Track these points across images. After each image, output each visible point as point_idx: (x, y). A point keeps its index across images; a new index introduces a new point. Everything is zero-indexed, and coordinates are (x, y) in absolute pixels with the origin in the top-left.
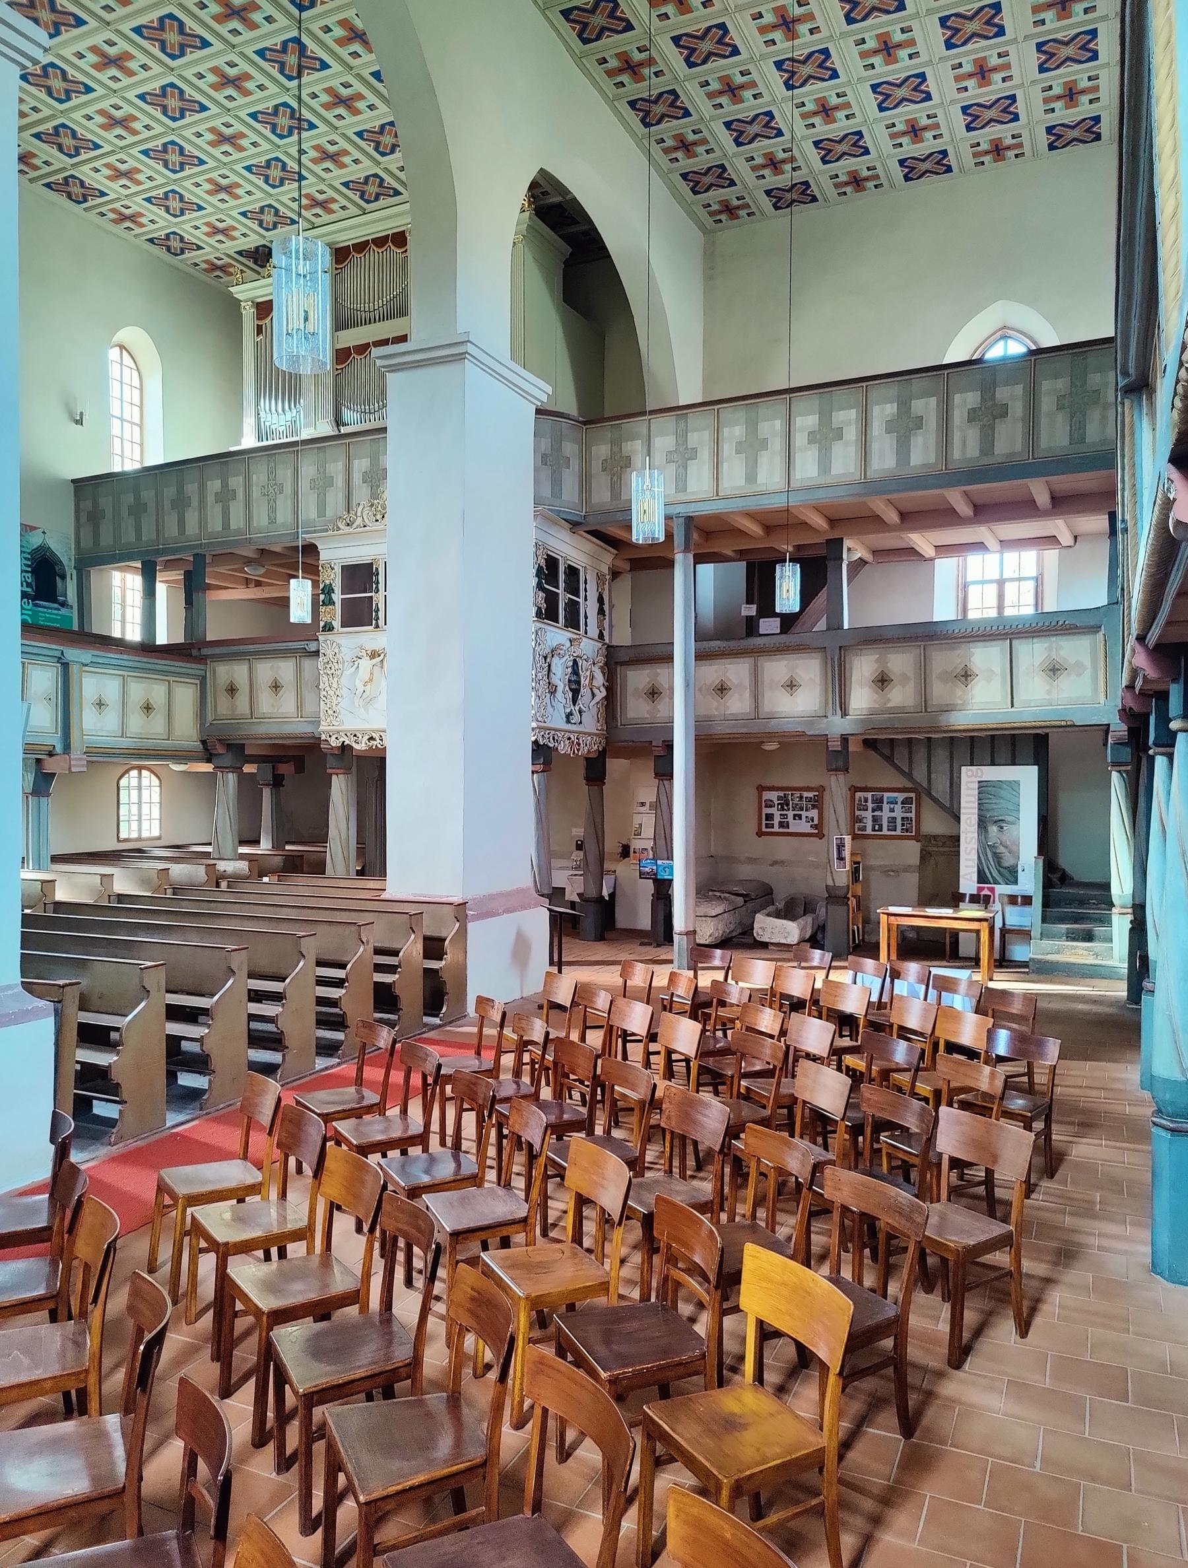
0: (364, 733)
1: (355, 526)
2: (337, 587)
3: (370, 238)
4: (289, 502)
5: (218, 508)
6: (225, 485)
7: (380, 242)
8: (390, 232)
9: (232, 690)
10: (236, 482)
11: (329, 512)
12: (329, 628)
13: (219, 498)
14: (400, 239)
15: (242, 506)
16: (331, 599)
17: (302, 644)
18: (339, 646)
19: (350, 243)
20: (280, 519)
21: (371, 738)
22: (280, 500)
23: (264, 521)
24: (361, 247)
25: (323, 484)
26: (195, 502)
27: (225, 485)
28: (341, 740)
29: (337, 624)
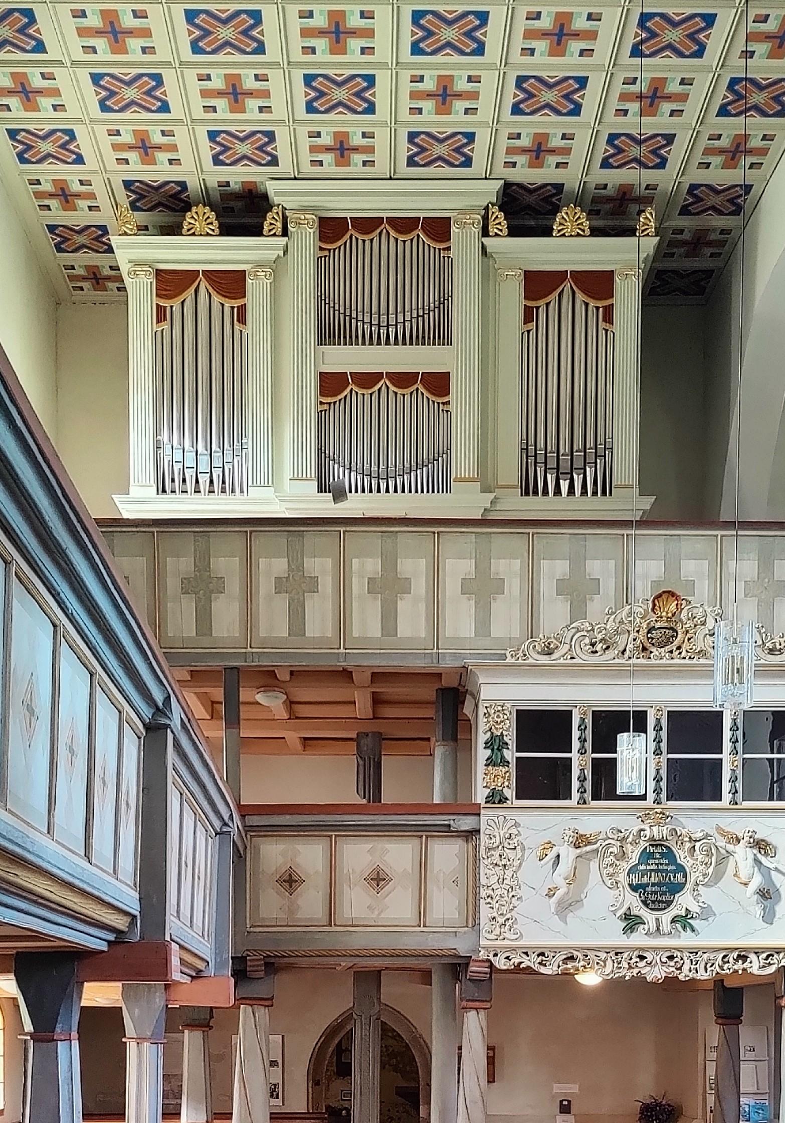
0: (556, 950)
1: (554, 656)
2: (511, 739)
3: (385, 215)
4: (422, 607)
5: (282, 603)
6: (295, 567)
7: (404, 225)
8: (422, 215)
9: (290, 881)
10: (319, 566)
11: (498, 630)
12: (496, 798)
13: (281, 585)
14: (439, 229)
15: (329, 606)
16: (503, 757)
17: (453, 822)
18: (517, 825)
19: (348, 215)
20: (404, 629)
21: (572, 958)
22: (403, 606)
23: (375, 630)
24: (367, 225)
25: (483, 589)
26: (234, 586)
27: (295, 567)
28: (517, 961)
29: (510, 793)
